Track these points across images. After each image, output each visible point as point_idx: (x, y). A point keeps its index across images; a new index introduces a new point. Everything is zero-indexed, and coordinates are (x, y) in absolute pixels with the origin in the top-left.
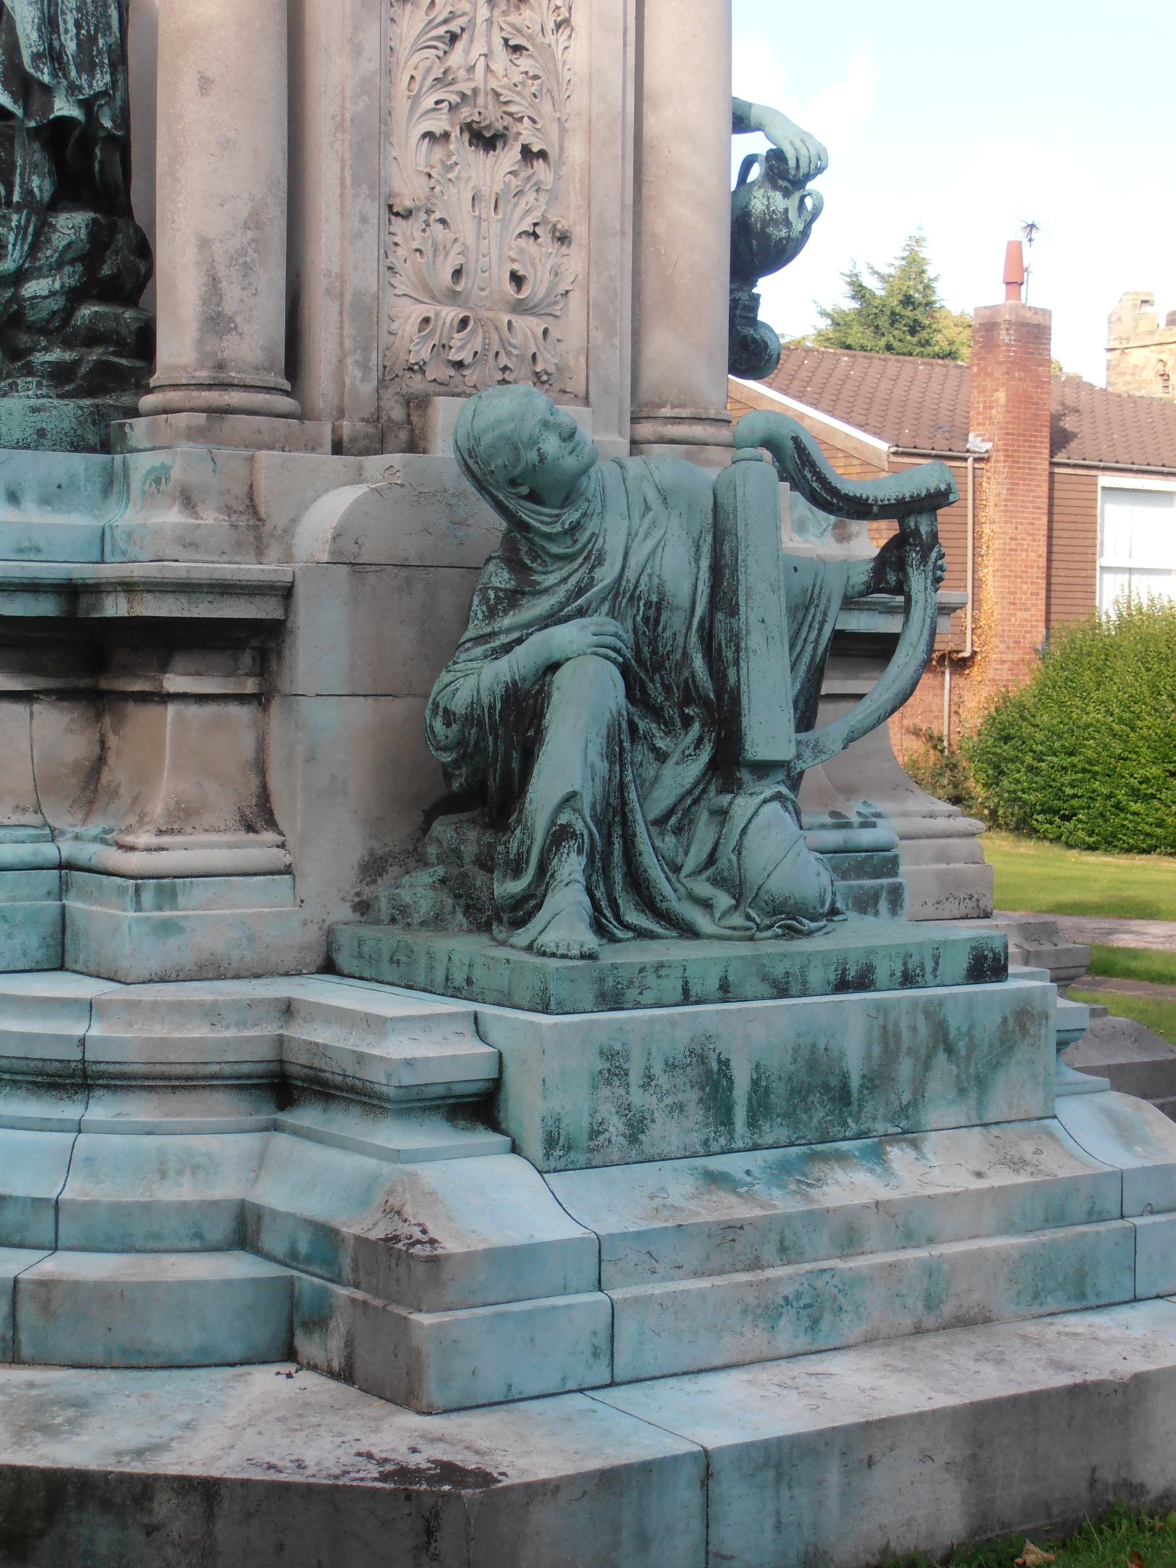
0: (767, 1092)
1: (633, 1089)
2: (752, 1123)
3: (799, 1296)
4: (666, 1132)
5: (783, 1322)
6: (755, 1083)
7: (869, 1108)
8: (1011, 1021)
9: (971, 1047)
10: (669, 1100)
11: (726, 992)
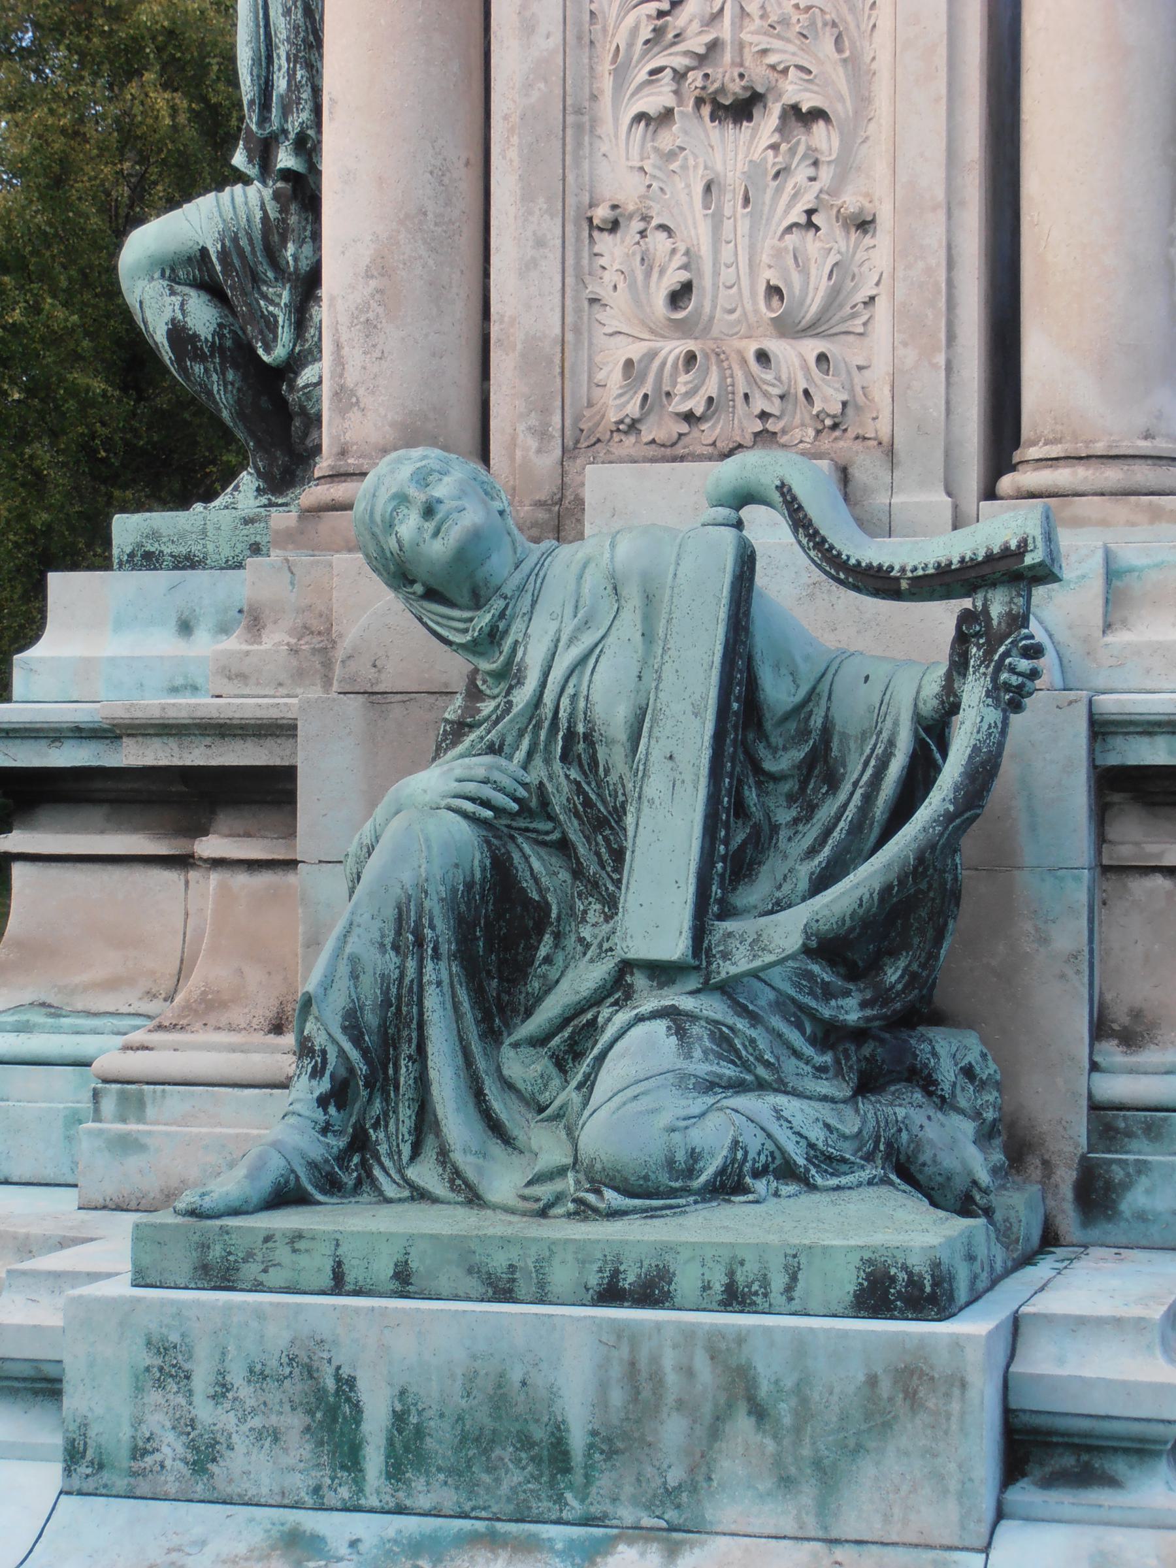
0: (420, 1432)
1: (198, 1399)
2: (395, 1472)
4: (246, 1463)
6: (399, 1418)
7: (604, 1482)
8: (885, 1387)
9: (804, 1413)
10: (256, 1422)
11: (404, 1282)
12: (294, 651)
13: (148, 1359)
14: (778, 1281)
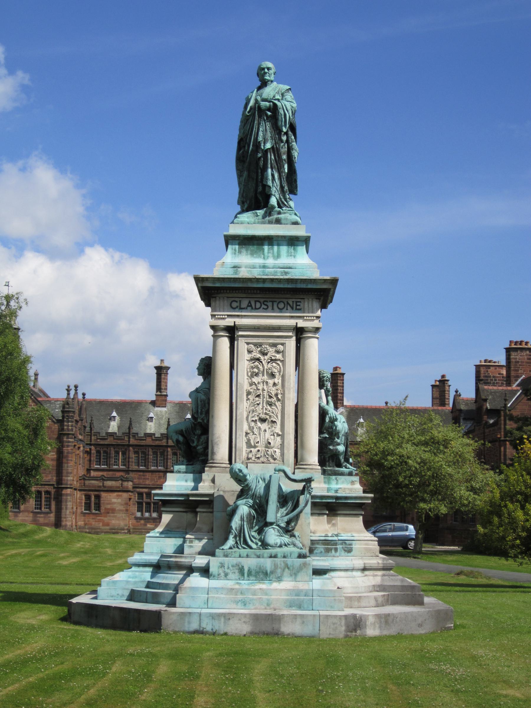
0: (251, 572)
2: (248, 576)
5: (239, 604)
6: (249, 570)
7: (271, 576)
9: (293, 568)
13: (220, 565)
14: (289, 555)
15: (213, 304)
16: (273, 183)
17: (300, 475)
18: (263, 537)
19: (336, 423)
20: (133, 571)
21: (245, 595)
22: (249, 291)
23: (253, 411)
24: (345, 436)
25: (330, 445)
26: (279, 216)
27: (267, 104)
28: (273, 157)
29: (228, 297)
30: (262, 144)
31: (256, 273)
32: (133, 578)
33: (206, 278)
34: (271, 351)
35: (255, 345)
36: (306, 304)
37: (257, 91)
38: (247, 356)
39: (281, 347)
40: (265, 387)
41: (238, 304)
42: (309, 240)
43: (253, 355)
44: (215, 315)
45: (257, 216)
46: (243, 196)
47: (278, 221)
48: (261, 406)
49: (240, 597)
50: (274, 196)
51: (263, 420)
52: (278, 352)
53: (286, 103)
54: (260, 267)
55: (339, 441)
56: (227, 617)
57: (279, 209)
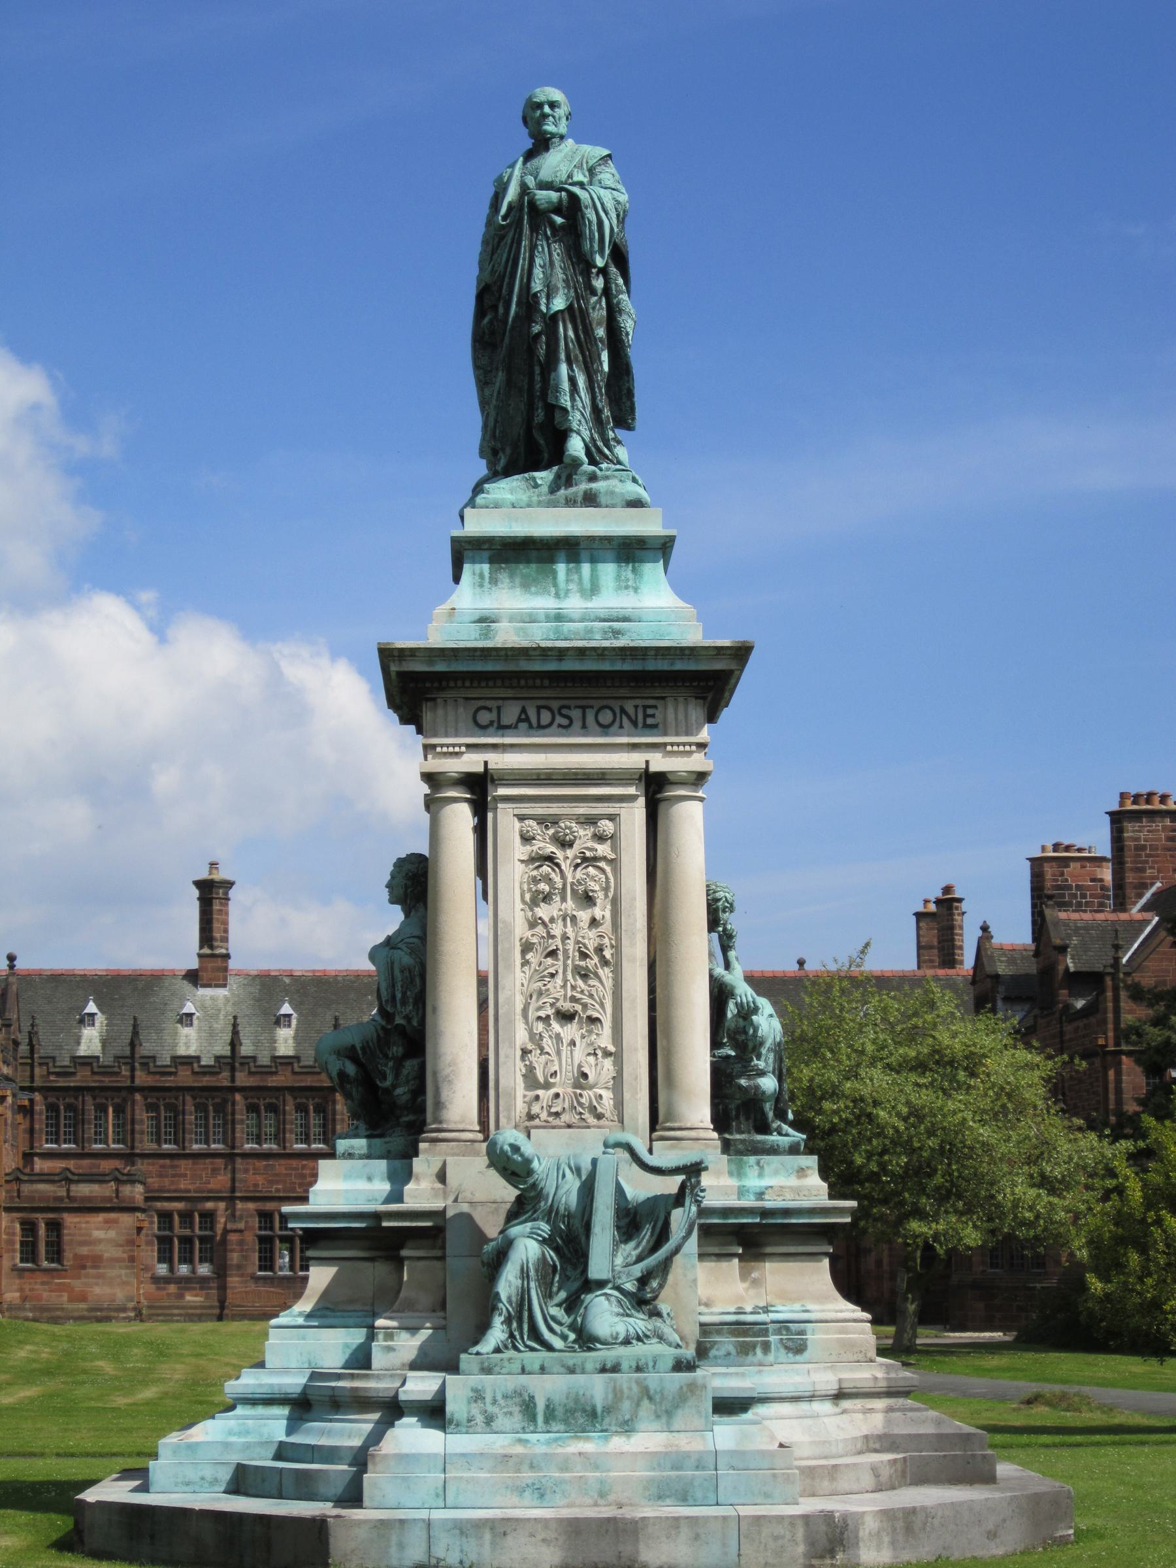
0: (553, 1410)
1: (488, 1404)
2: (547, 1421)
3: (533, 1484)
4: (501, 1422)
6: (547, 1407)
7: (607, 1420)
8: (685, 1389)
9: (663, 1398)
12: (433, 1189)
13: (471, 1394)
14: (651, 1364)
15: (427, 717)
16: (573, 399)
17: (665, 1156)
18: (579, 1320)
19: (754, 1018)
20: (238, 1418)
21: (540, 1470)
22: (523, 682)
23: (540, 994)
24: (775, 1052)
25: (739, 1077)
26: (593, 485)
27: (554, 195)
28: (571, 333)
29: (467, 699)
30: (543, 301)
31: (539, 635)
32: (239, 1434)
33: (411, 649)
34: (584, 835)
35: (542, 820)
36: (670, 712)
37: (525, 163)
38: (522, 851)
39: (607, 826)
40: (570, 931)
41: (493, 716)
42: (672, 547)
43: (535, 848)
44: (434, 746)
45: (536, 486)
46: (494, 436)
47: (590, 500)
48: (559, 980)
49: (528, 1476)
50: (578, 433)
51: (566, 1017)
52: (600, 838)
53: (602, 192)
54: (548, 619)
55: (761, 1064)
56: (500, 1529)
57: (592, 468)
